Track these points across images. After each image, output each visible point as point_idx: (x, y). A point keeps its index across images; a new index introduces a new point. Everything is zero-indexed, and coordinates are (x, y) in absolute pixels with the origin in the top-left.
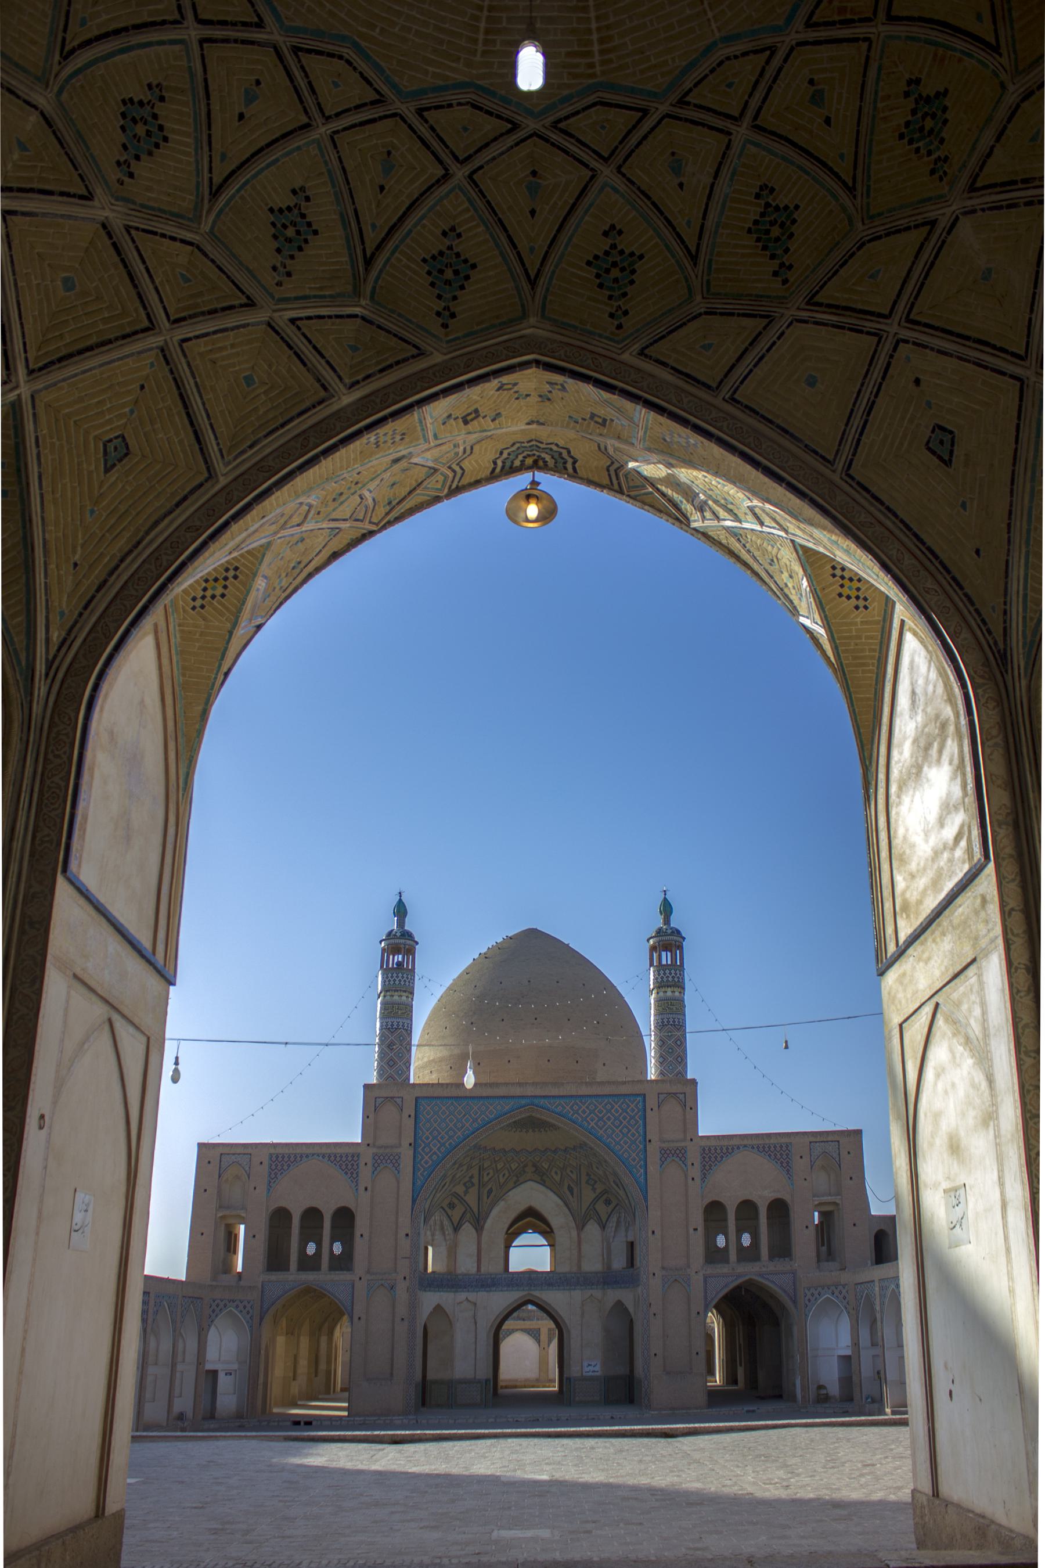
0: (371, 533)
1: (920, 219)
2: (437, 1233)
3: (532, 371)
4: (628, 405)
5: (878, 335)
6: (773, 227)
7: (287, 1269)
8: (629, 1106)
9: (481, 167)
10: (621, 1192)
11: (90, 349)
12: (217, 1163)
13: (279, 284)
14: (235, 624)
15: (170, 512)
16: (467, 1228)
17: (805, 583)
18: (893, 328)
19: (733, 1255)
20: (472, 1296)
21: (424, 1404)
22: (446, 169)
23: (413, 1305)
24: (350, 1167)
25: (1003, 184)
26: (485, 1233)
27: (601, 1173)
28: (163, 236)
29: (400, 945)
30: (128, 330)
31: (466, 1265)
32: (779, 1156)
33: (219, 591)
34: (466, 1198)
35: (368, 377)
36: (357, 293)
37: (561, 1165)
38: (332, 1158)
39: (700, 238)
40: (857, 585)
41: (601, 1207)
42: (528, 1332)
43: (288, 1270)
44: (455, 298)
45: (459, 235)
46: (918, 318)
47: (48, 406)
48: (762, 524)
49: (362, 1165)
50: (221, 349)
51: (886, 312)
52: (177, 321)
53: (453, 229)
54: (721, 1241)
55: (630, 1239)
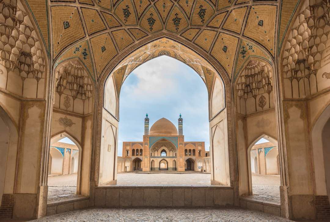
0: (141, 64)
1: (226, 10)
3: (165, 38)
4: (178, 44)
5: (217, 31)
6: (202, 13)
7: (134, 155)
9: (156, 2)
11: (98, 32)
12: (125, 144)
13: (126, 23)
14: (124, 76)
15: (113, 59)
17: (202, 71)
18: (220, 30)
19: (188, 155)
21: (151, 170)
22: (150, 3)
23: (150, 160)
25: (241, 4)
28: (107, 13)
29: (147, 120)
30: (103, 29)
31: (156, 155)
33: (121, 71)
35: (140, 39)
36: (137, 25)
39: (190, 15)
40: (209, 71)
41: (172, 150)
42: (163, 163)
44: (152, 26)
45: (153, 15)
46: (224, 28)
47: (92, 41)
48: (197, 63)
50: (118, 33)
51: (219, 27)
52: (110, 28)
53: (152, 14)
54: (187, 154)
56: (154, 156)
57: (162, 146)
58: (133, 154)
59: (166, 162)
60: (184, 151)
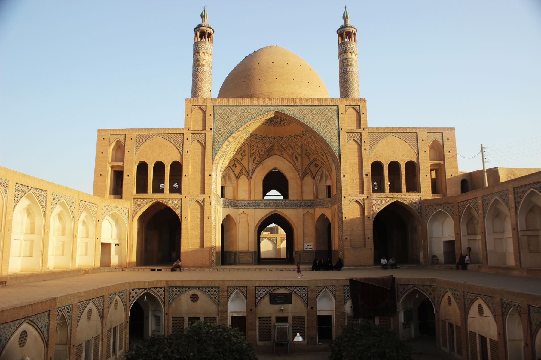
2: (227, 180)
8: (329, 111)
10: (325, 158)
16: (243, 178)
20: (246, 211)
24: (178, 140)
26: (252, 180)
27: (314, 148)
31: (243, 195)
32: (411, 139)
34: (242, 162)
37: (292, 145)
38: (169, 136)
41: (312, 168)
43: (146, 193)
49: (185, 139)
55: (329, 183)
56: (234, 199)
57: (269, 153)
58: (141, 188)
59: (282, 232)
60: (367, 169)
